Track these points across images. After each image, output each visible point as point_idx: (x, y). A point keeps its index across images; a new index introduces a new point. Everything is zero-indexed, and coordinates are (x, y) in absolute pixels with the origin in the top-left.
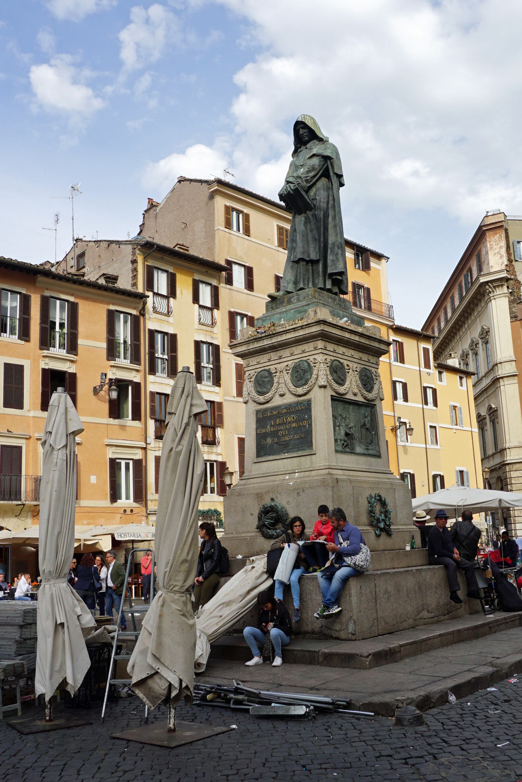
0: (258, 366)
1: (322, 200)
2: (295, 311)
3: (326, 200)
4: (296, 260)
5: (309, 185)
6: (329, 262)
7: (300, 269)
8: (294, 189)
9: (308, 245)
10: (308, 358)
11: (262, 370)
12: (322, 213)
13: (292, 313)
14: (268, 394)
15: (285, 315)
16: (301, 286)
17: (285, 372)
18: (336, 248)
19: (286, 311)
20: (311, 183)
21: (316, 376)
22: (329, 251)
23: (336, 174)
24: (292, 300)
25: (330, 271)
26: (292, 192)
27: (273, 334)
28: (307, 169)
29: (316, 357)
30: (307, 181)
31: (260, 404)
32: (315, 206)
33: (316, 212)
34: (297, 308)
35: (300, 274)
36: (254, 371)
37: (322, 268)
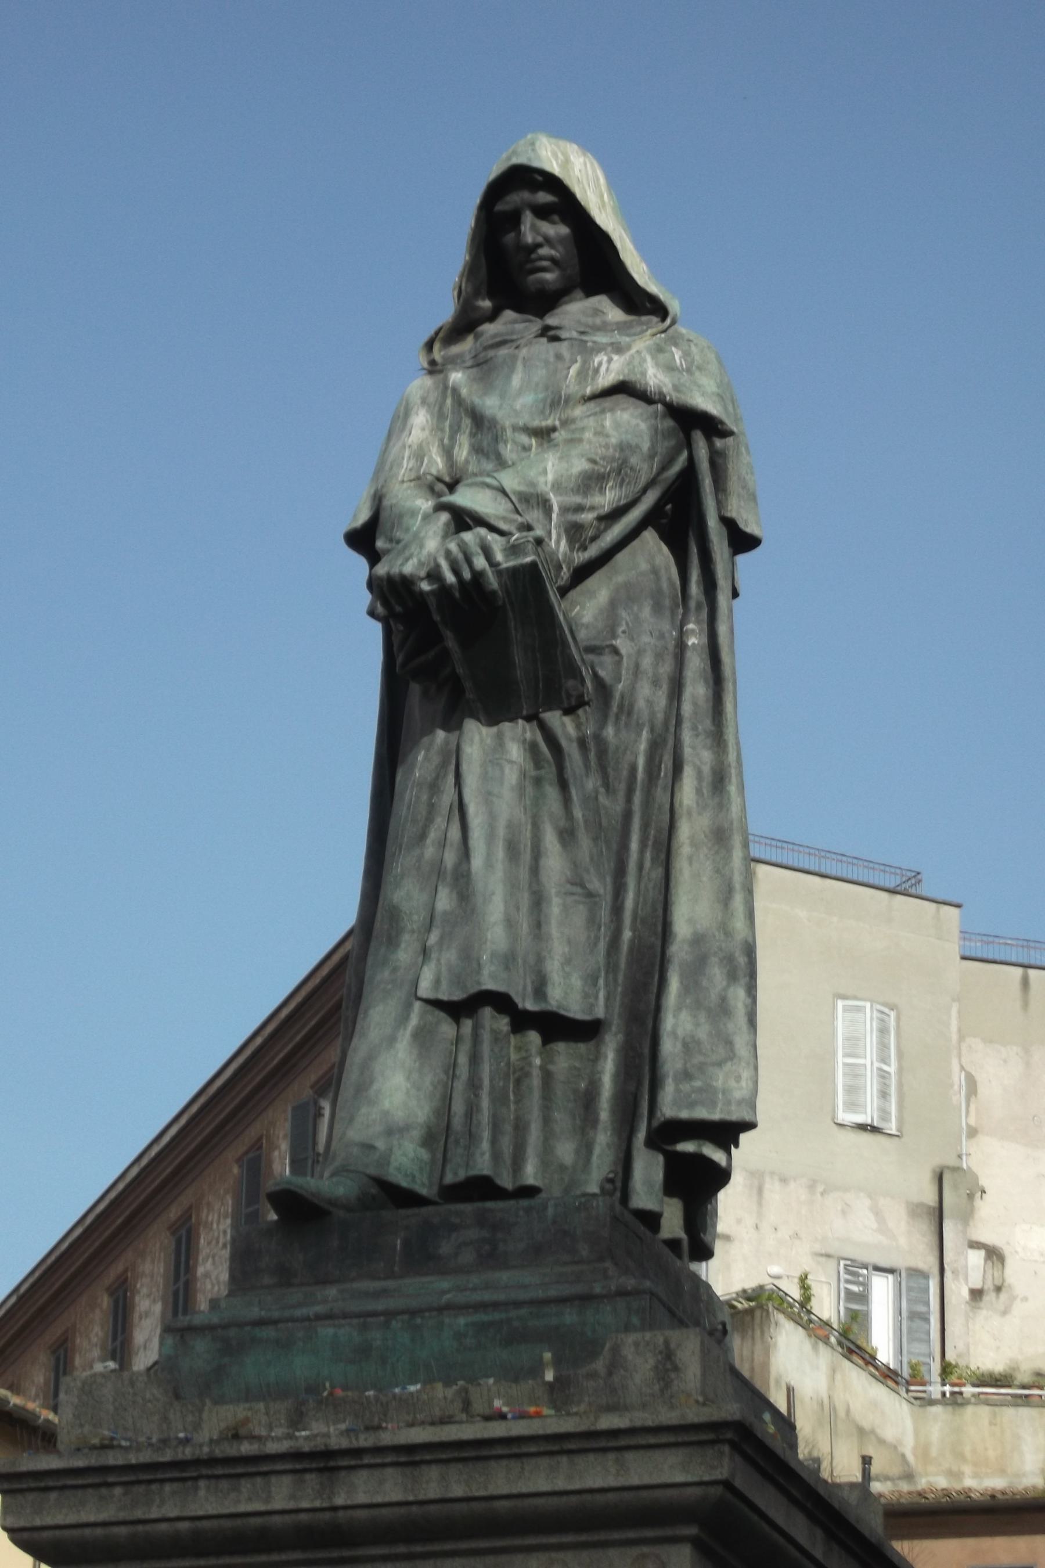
1: (647, 662)
3: (666, 668)
4: (457, 996)
5: (581, 557)
6: (669, 1047)
7: (475, 1059)
8: (514, 573)
9: (538, 925)
12: (643, 746)
16: (483, 1164)
18: (717, 973)
19: (413, 1313)
20: (593, 551)
22: (674, 985)
23: (730, 525)
24: (445, 1248)
25: (670, 1107)
26: (493, 582)
27: (357, 1452)
28: (586, 466)
30: (575, 532)
32: (601, 685)
33: (610, 732)
34: (495, 1305)
35: (474, 1085)
37: (616, 1076)
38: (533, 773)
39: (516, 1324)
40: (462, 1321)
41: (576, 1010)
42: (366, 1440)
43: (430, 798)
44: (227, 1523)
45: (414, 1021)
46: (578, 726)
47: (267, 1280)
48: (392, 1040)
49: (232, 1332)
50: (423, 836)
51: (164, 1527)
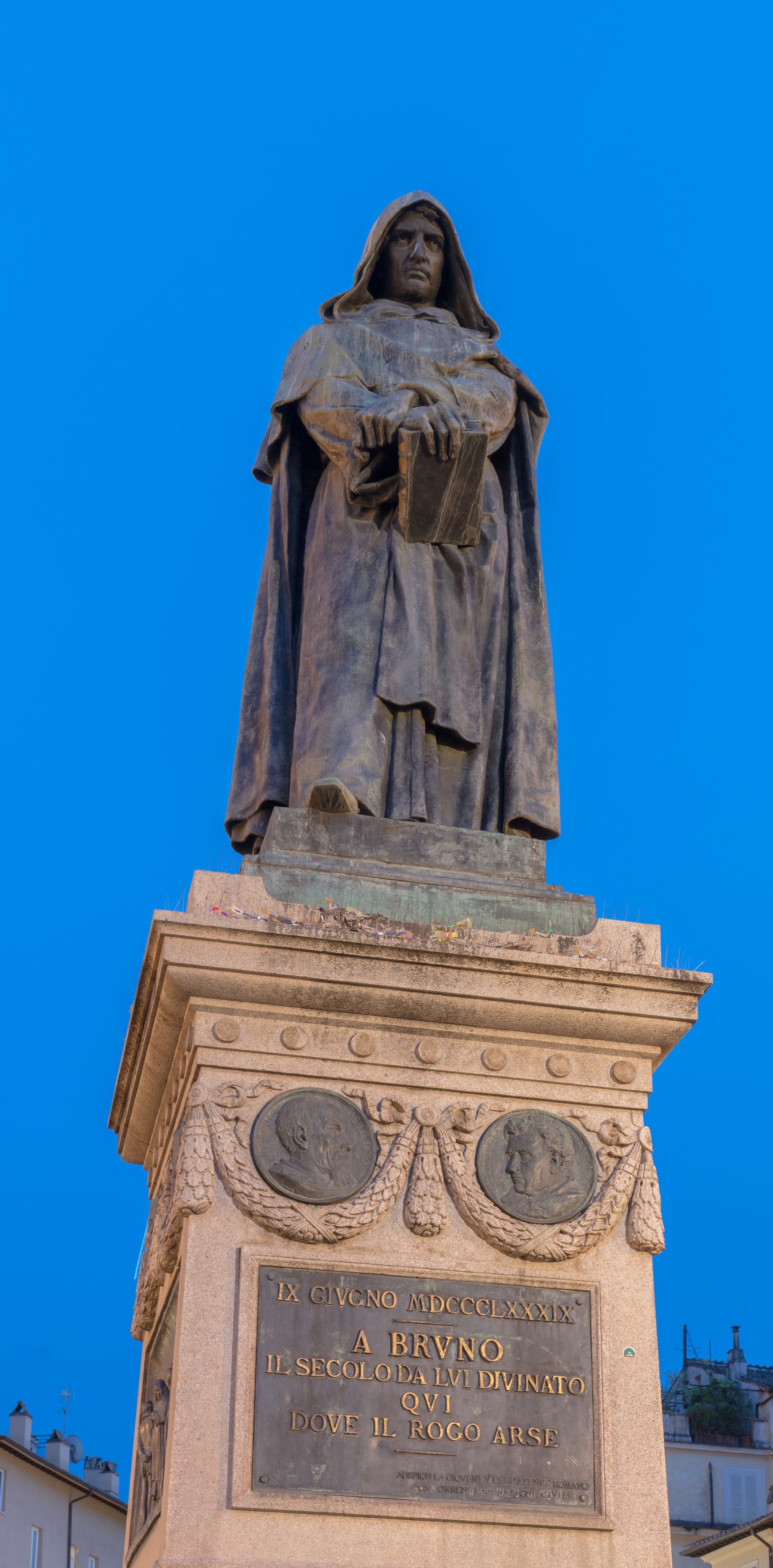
0: (283, 1064)
2: (480, 903)
4: (400, 701)
7: (409, 743)
10: (578, 1111)
11: (313, 1091)
13: (462, 904)
14: (349, 1209)
15: (424, 898)
17: (448, 1138)
19: (430, 885)
21: (624, 1200)
24: (432, 850)
29: (623, 1118)
31: (289, 1236)
36: (256, 1079)
38: (437, 580)
39: (503, 905)
40: (465, 896)
41: (465, 733)
42: (453, 949)
43: (371, 576)
44: (337, 988)
45: (374, 710)
46: (467, 559)
47: (301, 847)
48: (362, 719)
49: (297, 872)
50: (368, 597)
51: (292, 982)
